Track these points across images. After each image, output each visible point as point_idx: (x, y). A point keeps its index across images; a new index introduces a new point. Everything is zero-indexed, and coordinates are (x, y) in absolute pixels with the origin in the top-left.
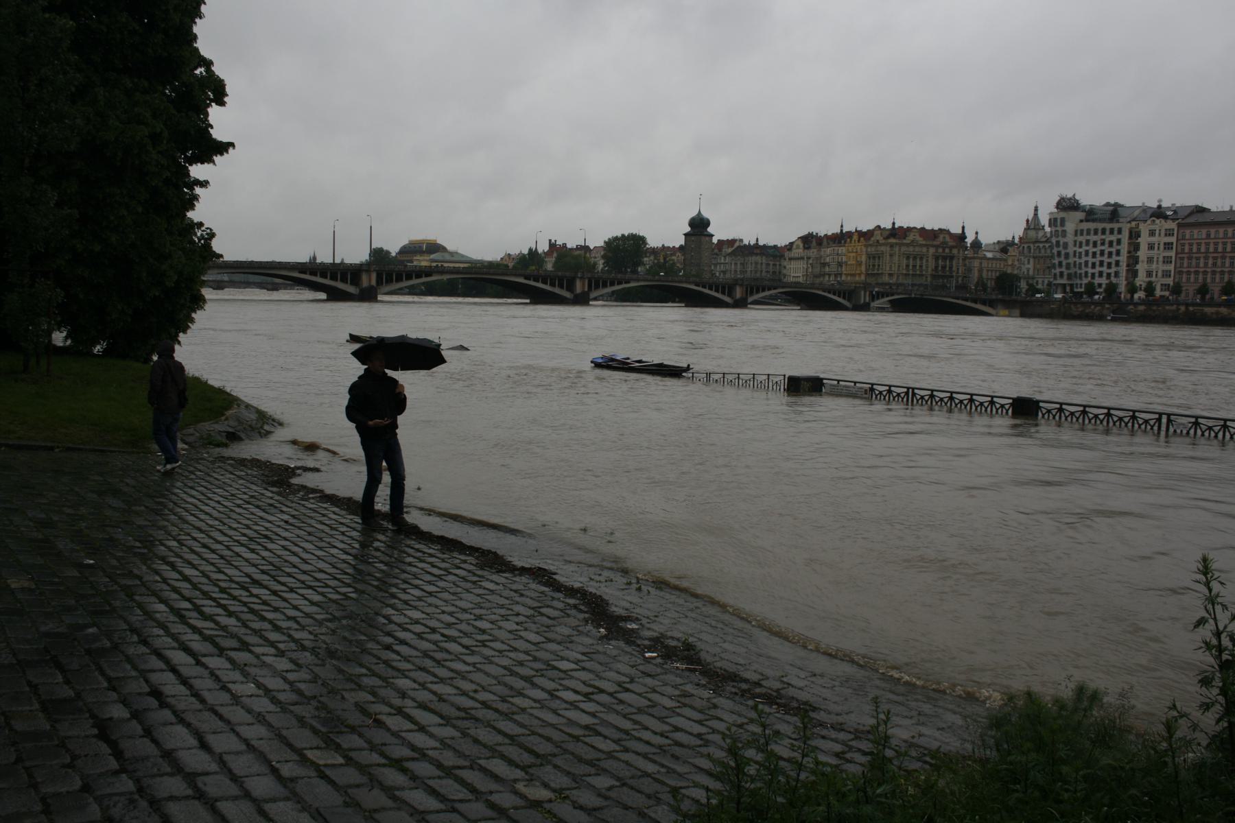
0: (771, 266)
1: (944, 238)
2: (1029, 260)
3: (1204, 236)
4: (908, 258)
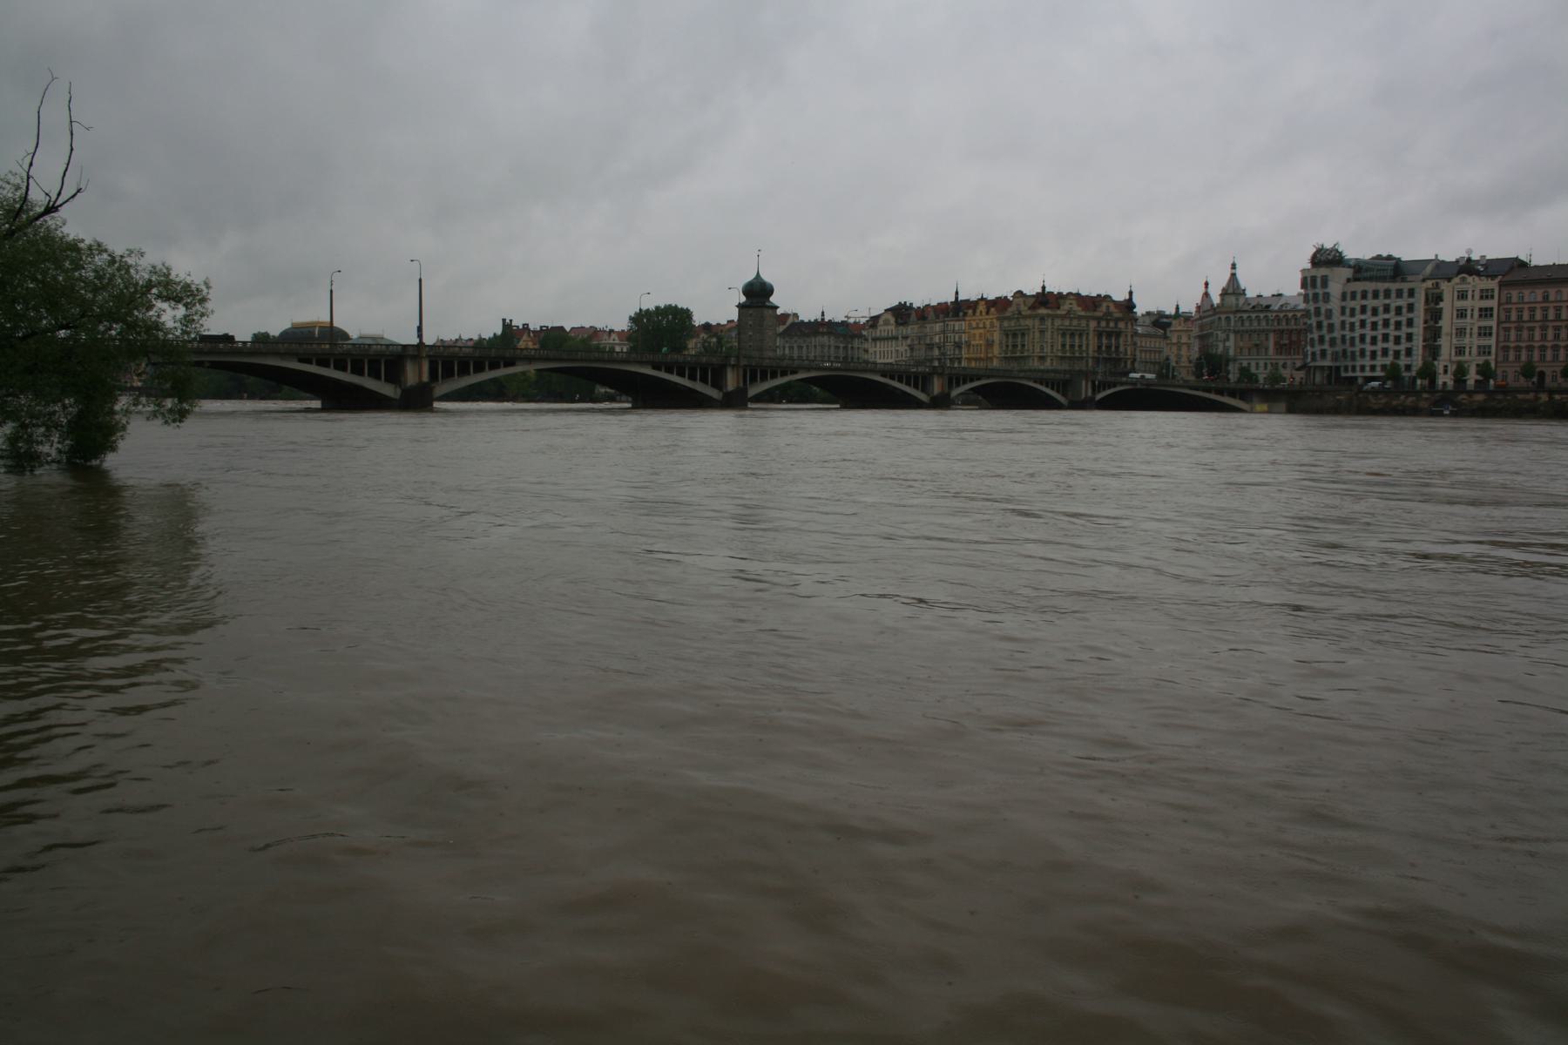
0: (841, 349)
1: (1108, 307)
3: (1540, 298)
4: (1064, 335)
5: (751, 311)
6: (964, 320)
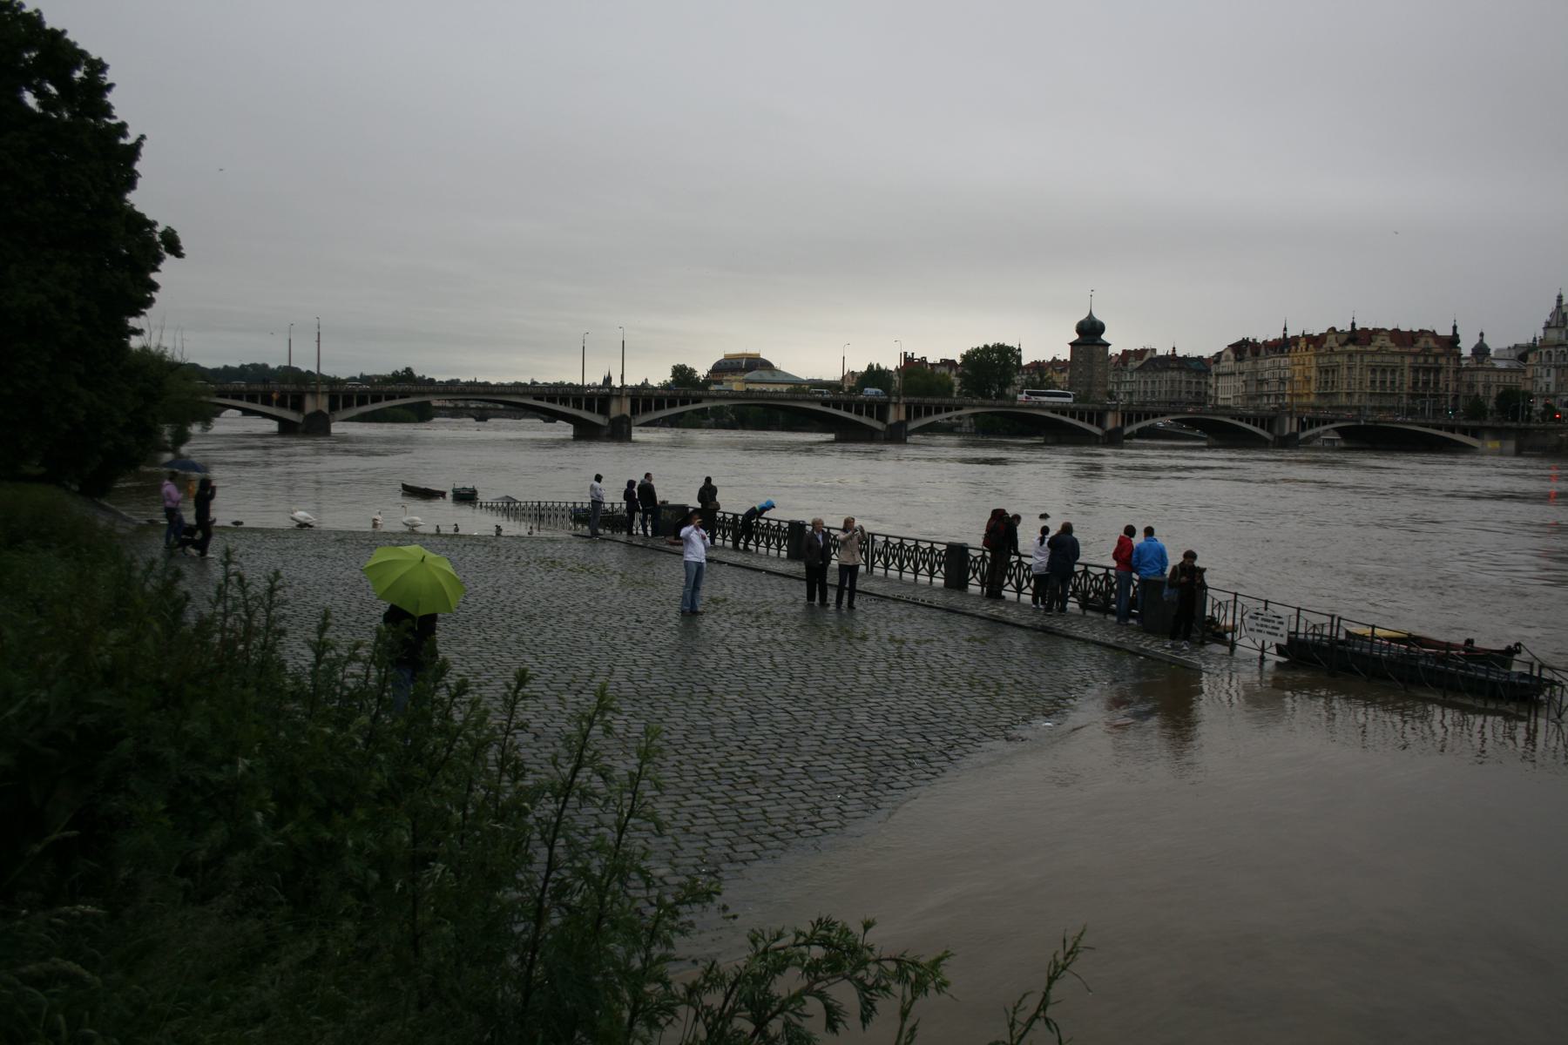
1: (1427, 342)
2: (1549, 371)
4: (1374, 371)
6: (1288, 356)
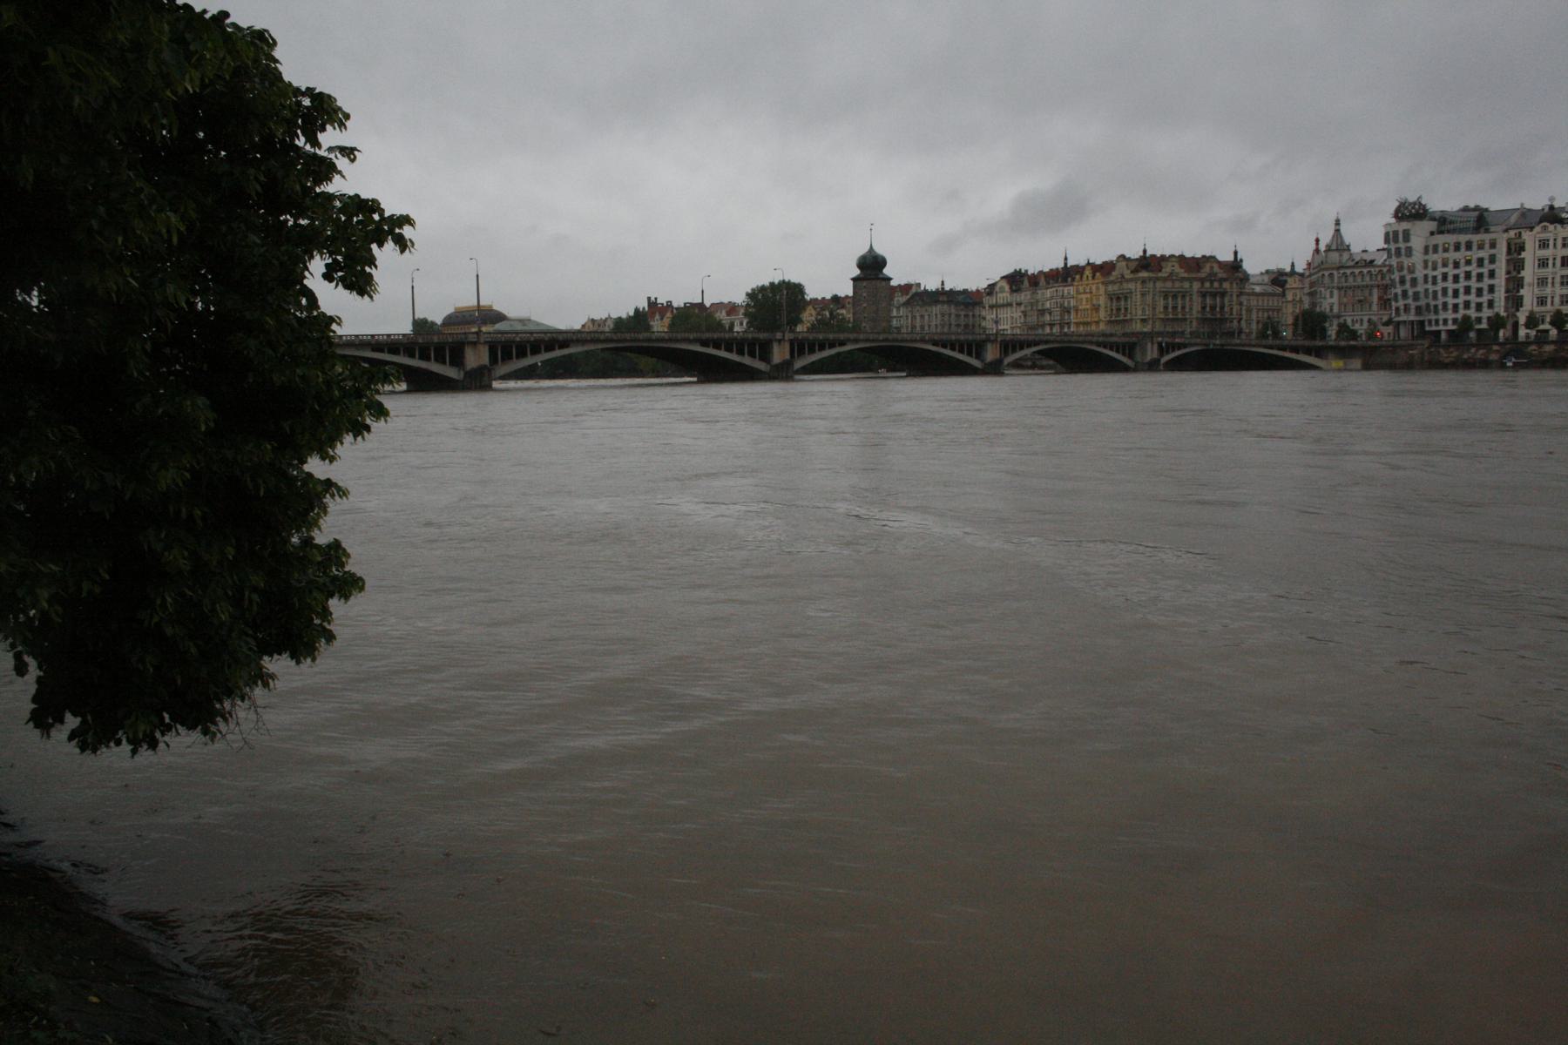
1: (1212, 268)
2: (1331, 293)
4: (1166, 297)
5: (865, 284)
6: (1072, 285)
